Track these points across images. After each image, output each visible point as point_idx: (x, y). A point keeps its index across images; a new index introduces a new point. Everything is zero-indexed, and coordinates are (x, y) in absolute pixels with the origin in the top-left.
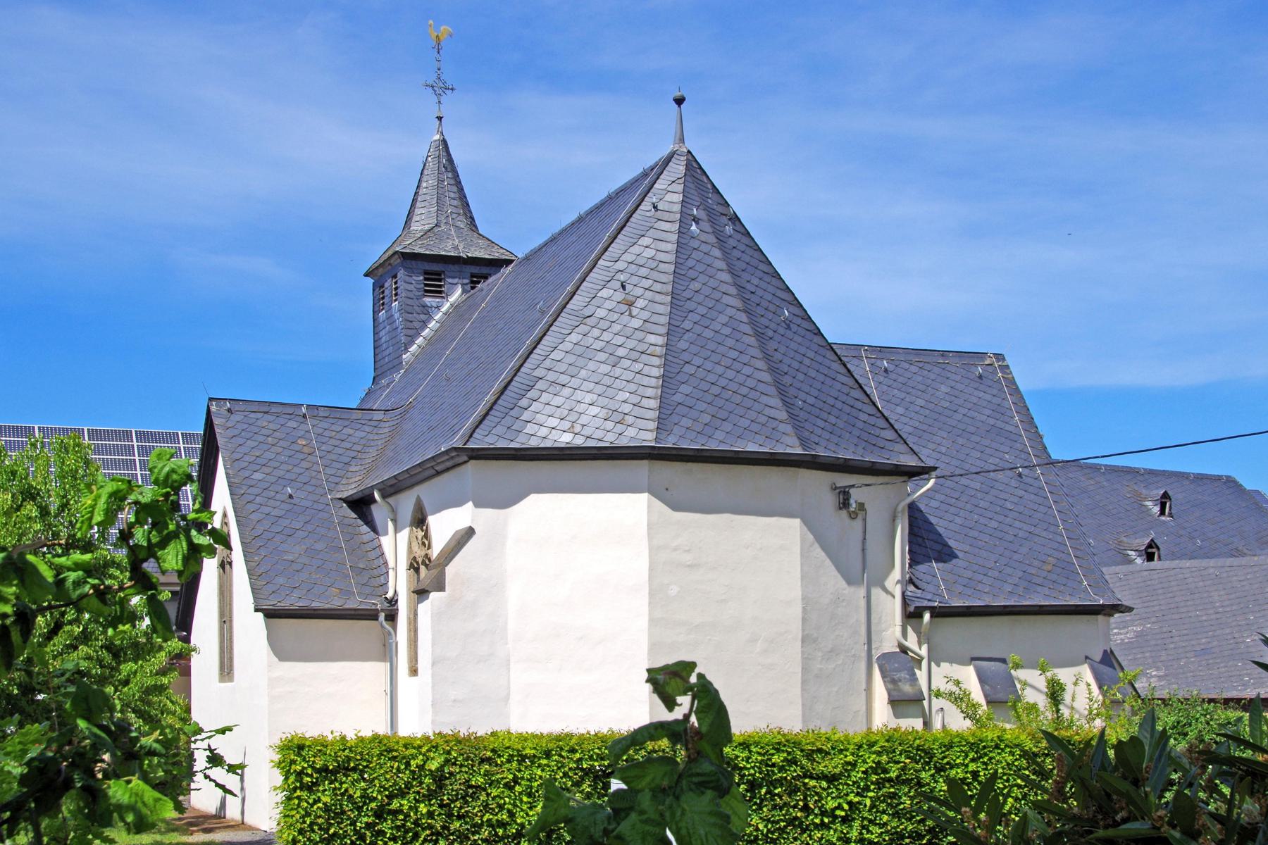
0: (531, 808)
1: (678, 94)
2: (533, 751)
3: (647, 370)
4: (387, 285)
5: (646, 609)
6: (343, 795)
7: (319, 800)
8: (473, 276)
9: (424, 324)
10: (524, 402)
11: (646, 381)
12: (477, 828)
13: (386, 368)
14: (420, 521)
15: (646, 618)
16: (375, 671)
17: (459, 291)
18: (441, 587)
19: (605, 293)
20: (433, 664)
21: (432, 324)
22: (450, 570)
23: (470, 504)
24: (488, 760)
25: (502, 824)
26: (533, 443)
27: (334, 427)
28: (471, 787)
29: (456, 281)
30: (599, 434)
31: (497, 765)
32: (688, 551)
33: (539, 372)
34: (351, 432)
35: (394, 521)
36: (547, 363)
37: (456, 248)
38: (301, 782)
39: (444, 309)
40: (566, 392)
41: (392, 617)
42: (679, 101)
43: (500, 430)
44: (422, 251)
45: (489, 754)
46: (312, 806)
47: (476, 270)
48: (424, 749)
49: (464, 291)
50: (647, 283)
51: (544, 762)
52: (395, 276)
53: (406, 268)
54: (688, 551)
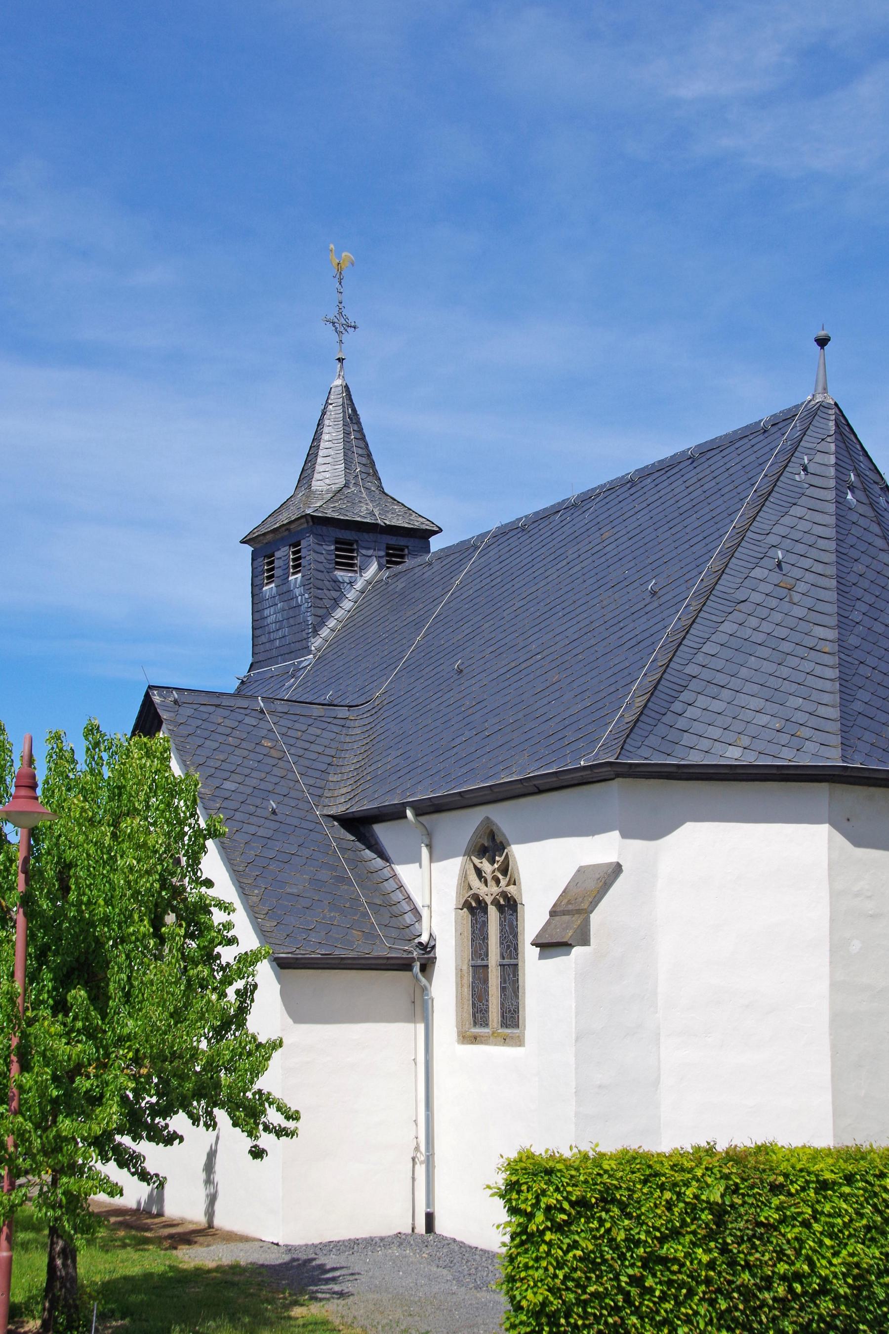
0: (836, 1254)
1: (822, 333)
2: (833, 1176)
3: (819, 670)
4: (278, 554)
5: (826, 970)
6: (602, 1236)
7: (575, 1245)
8: (388, 547)
9: (336, 603)
10: (677, 707)
11: (820, 684)
12: (768, 1283)
13: (274, 653)
14: (490, 846)
15: (827, 983)
16: (403, 1035)
17: (374, 567)
18: (585, 941)
19: (758, 573)
20: (577, 1040)
21: (347, 605)
22: (595, 918)
23: (616, 834)
24: (776, 1189)
25: (798, 1277)
26: (695, 758)
27: (297, 726)
28: (760, 1224)
29: (370, 552)
30: (772, 749)
31: (790, 1194)
32: (869, 897)
33: (692, 669)
34: (319, 732)
35: (429, 846)
36: (700, 658)
37: (372, 514)
38: (552, 1220)
39: (359, 585)
40: (726, 694)
41: (427, 966)
42: (822, 342)
43: (653, 740)
44: (335, 515)
45: (781, 1179)
46: (565, 1253)
47: (393, 541)
48: (699, 1172)
49: (380, 568)
50: (807, 563)
51: (847, 1190)
52: (297, 544)
53: (316, 535)
54: (869, 897)
